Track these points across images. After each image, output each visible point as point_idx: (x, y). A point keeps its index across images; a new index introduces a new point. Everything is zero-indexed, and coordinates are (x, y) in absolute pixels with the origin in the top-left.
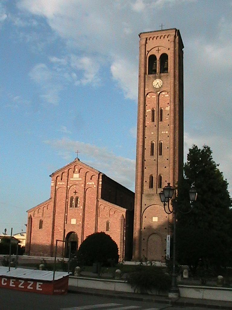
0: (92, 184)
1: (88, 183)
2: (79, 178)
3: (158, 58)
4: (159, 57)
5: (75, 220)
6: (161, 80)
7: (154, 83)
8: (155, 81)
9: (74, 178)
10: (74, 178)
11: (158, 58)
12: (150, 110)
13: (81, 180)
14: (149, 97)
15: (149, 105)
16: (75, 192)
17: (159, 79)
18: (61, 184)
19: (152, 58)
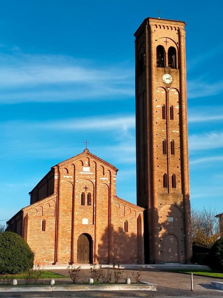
0: (106, 180)
1: (100, 179)
2: (91, 172)
3: (166, 50)
4: (168, 50)
5: (87, 220)
6: (170, 76)
7: (163, 77)
8: (165, 75)
9: (84, 172)
10: (84, 172)
11: (166, 50)
12: (160, 106)
13: (92, 174)
14: (159, 92)
15: (159, 100)
16: (86, 188)
17: (169, 75)
18: (68, 178)
19: (160, 49)
